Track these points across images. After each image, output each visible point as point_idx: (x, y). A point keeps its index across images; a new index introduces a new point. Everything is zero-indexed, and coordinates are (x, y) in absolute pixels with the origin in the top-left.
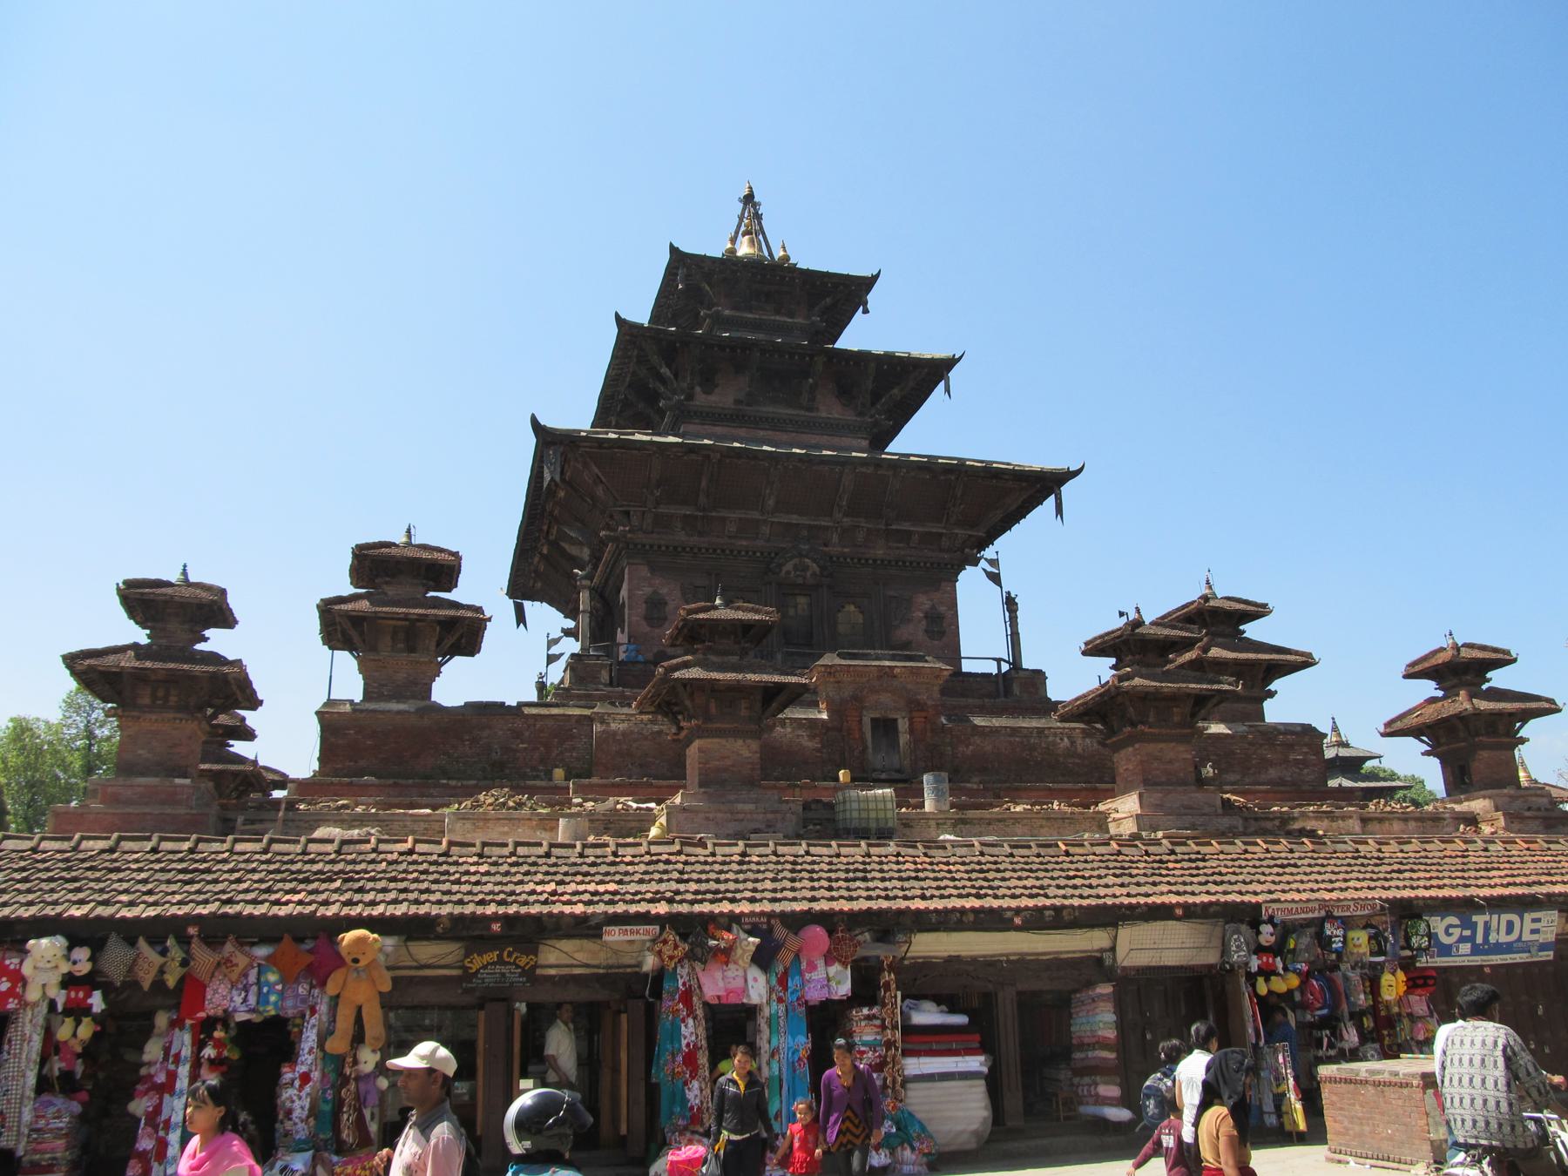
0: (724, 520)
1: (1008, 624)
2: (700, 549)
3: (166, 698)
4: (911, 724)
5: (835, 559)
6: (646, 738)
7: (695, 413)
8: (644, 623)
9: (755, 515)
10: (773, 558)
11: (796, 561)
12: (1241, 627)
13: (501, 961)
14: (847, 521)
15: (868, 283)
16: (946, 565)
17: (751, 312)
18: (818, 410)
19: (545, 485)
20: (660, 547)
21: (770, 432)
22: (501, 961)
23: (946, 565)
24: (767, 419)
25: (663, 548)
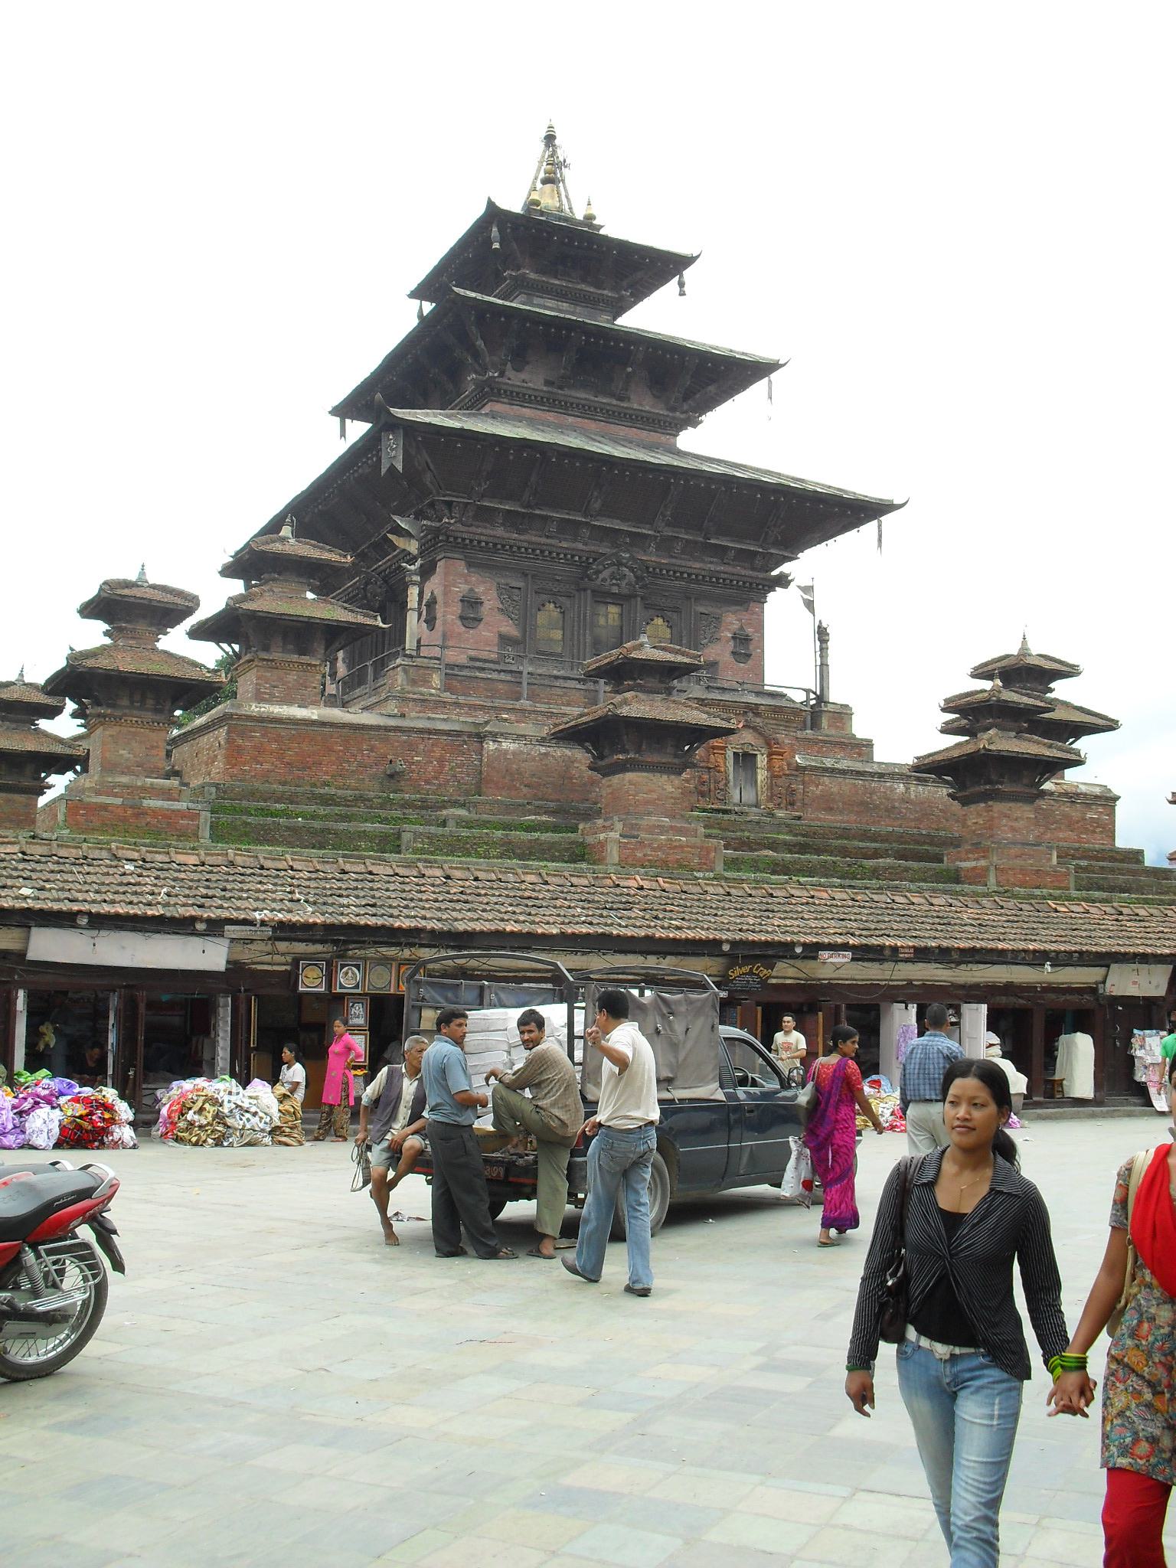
0: (545, 518)
1: (818, 653)
3: (143, 701)
4: (770, 761)
5: (651, 569)
6: (534, 760)
7: (505, 391)
8: (459, 623)
10: (588, 566)
11: (613, 569)
12: (1052, 685)
13: (751, 973)
14: (668, 532)
16: (758, 585)
17: (556, 278)
18: (629, 399)
19: (383, 471)
20: (479, 542)
21: (579, 419)
22: (751, 973)
23: (758, 585)
24: (578, 405)
25: (483, 544)
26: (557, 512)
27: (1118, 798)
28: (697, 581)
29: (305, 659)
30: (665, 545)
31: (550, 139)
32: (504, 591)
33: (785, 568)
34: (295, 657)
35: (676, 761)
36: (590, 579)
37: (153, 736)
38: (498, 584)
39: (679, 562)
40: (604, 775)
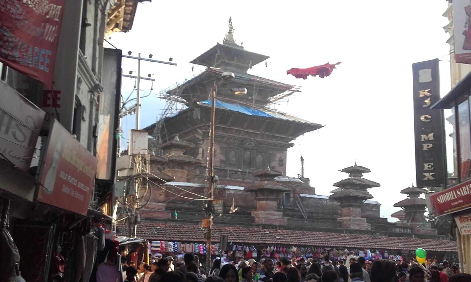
0: (232, 129)
2: (226, 137)
9: (240, 129)
15: (268, 57)
26: (235, 128)
27: (381, 205)
28: (270, 145)
29: (183, 170)
30: (262, 135)
31: (230, 20)
32: (222, 148)
33: (293, 142)
34: (180, 170)
35: (276, 198)
36: (243, 145)
37: (156, 192)
38: (220, 146)
39: (266, 140)
40: (258, 201)
